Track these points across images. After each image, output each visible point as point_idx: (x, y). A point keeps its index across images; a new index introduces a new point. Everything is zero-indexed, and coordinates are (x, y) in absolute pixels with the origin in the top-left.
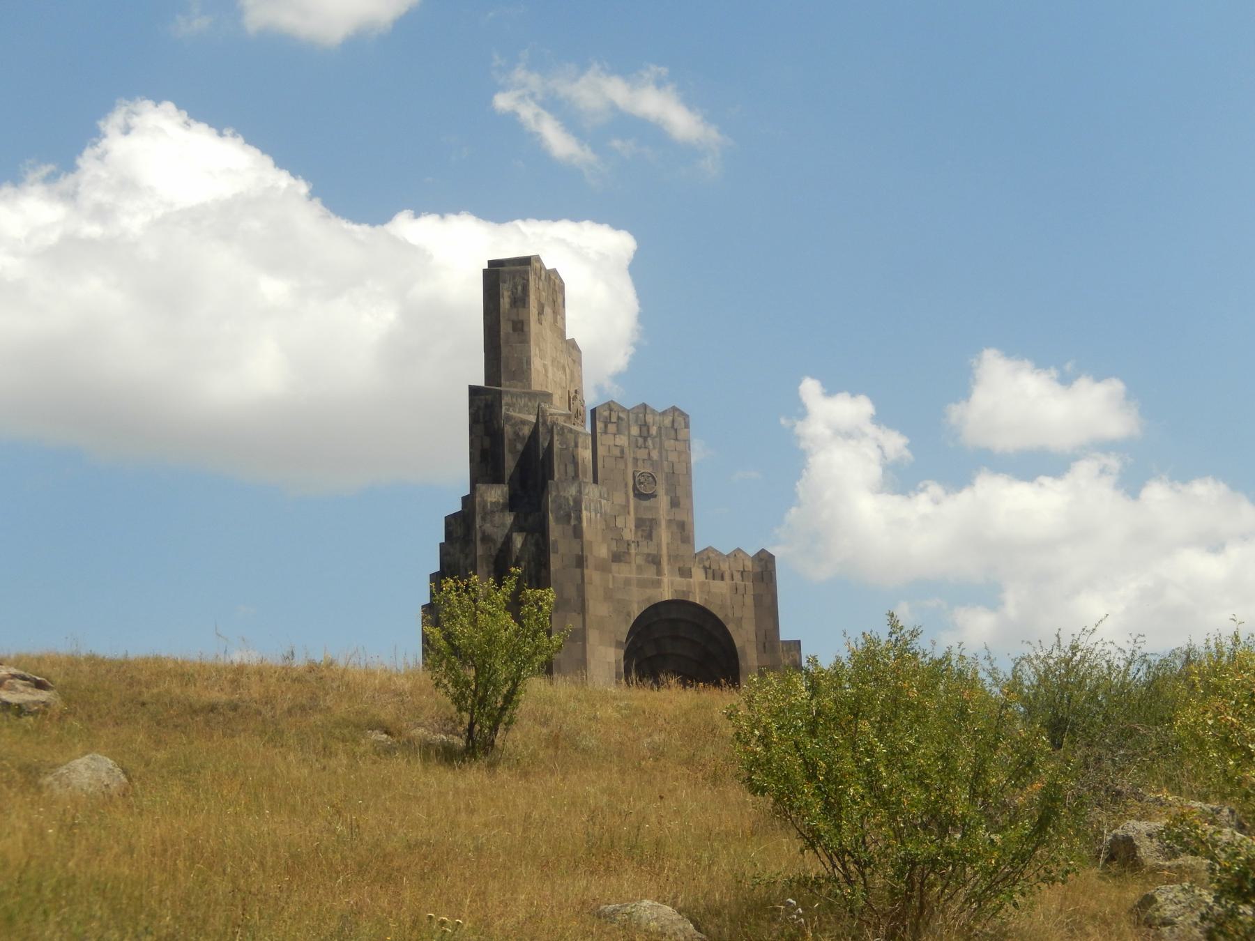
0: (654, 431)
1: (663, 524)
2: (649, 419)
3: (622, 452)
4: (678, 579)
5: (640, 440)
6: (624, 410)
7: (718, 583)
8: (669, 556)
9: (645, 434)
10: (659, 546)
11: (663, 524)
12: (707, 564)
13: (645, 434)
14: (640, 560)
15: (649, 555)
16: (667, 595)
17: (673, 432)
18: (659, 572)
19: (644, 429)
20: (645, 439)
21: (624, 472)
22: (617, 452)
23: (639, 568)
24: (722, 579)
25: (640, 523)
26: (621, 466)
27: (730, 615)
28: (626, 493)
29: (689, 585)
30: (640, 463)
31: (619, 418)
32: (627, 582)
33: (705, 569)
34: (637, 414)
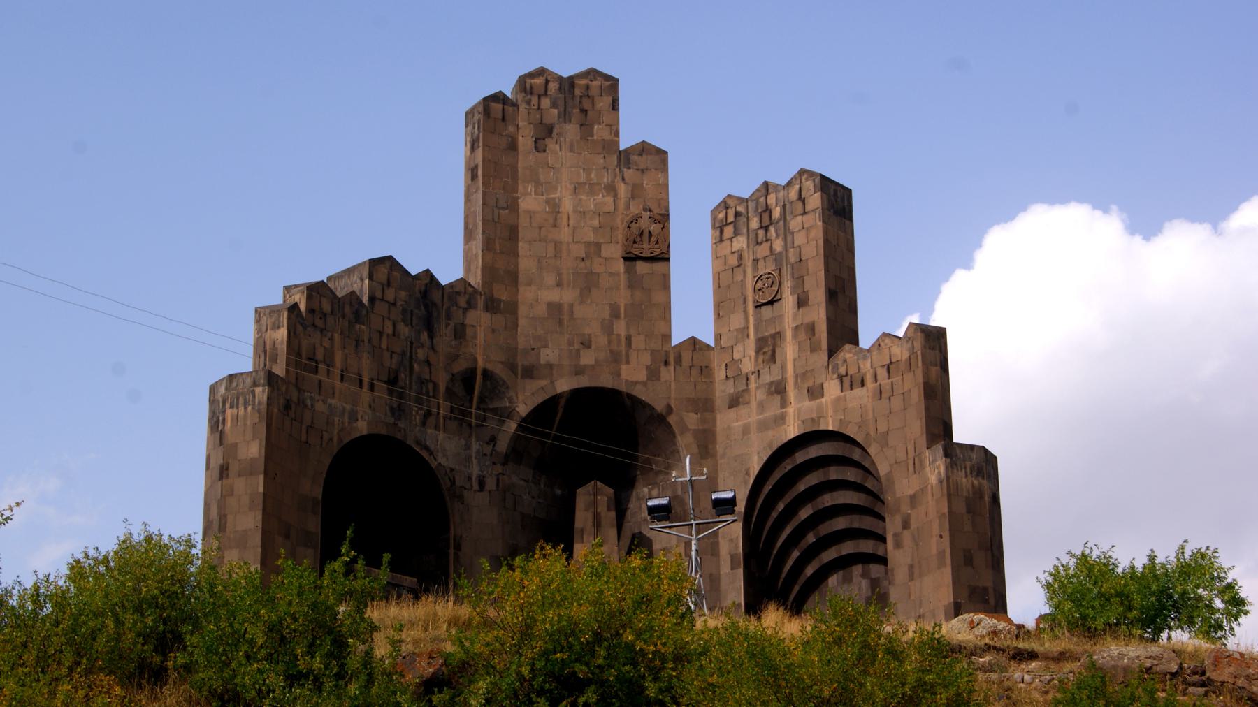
0: (777, 213)
1: (789, 334)
2: (772, 199)
3: (740, 257)
4: (807, 404)
5: (761, 232)
6: (741, 200)
7: (858, 392)
8: (797, 376)
9: (766, 222)
10: (783, 368)
11: (789, 334)
12: (842, 371)
13: (766, 222)
14: (761, 395)
15: (772, 383)
16: (792, 431)
17: (800, 204)
18: (784, 404)
19: (766, 216)
20: (766, 229)
21: (743, 284)
22: (733, 261)
23: (762, 407)
24: (863, 384)
25: (761, 343)
26: (739, 277)
27: (872, 433)
28: (745, 312)
29: (820, 408)
30: (761, 263)
31: (737, 214)
32: (746, 430)
33: (841, 378)
34: (757, 201)
